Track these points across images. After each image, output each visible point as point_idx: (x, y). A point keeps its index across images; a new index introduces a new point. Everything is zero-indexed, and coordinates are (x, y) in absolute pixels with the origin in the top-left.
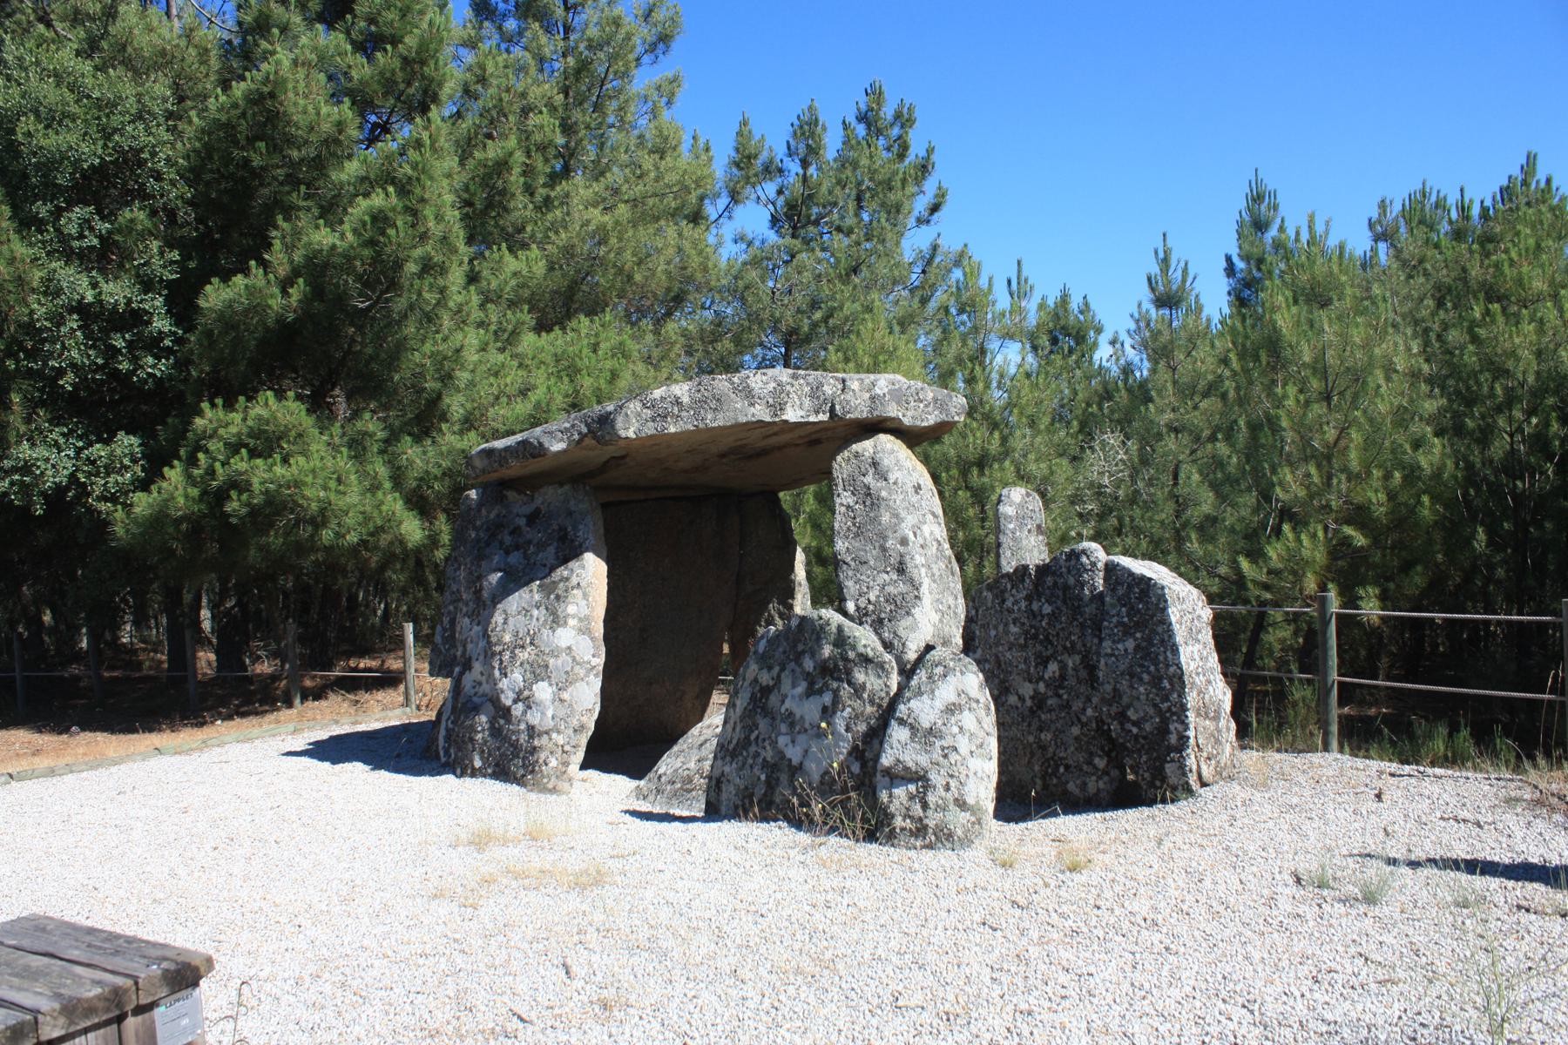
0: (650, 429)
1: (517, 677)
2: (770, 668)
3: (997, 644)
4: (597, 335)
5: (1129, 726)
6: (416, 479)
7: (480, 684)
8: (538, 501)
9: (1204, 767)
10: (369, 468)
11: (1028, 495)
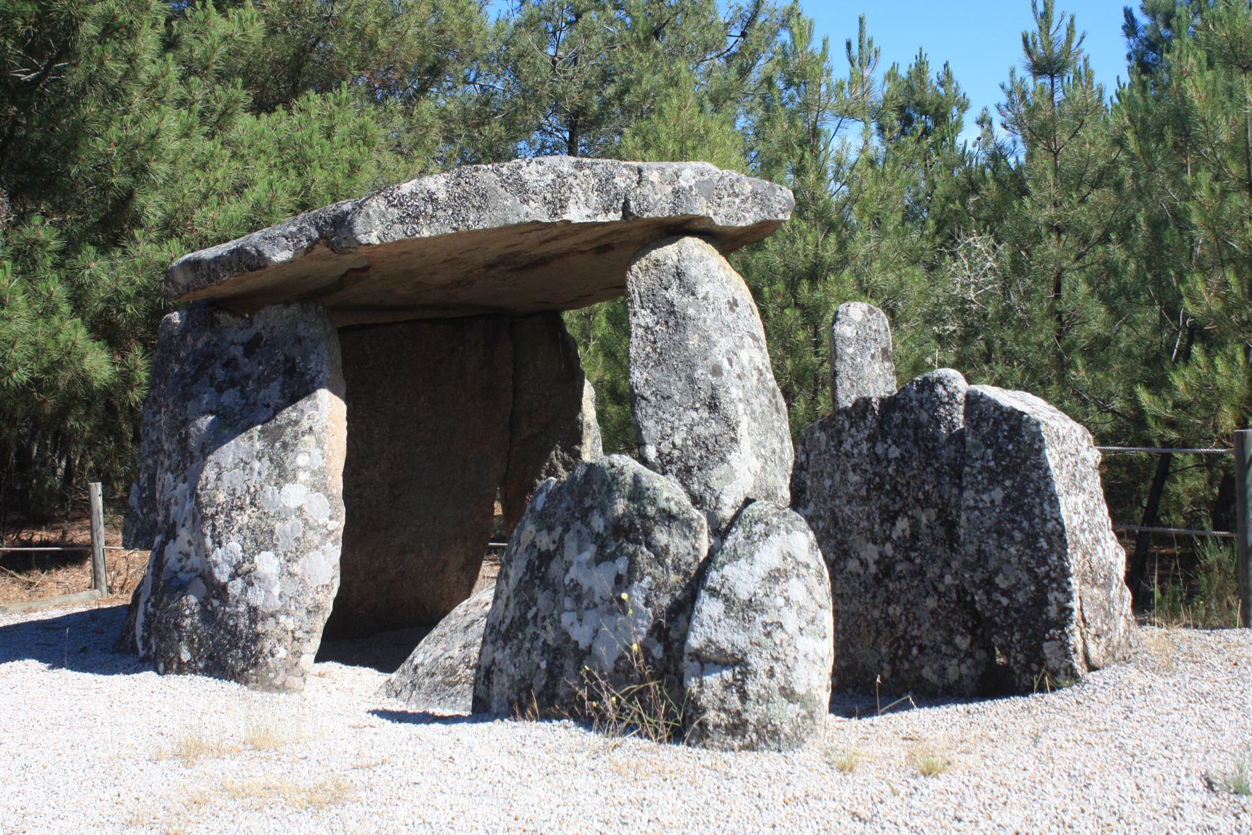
0: (398, 233)
1: (234, 546)
2: (550, 529)
3: (834, 497)
4: (331, 117)
5: (997, 596)
6: (102, 300)
7: (188, 556)
8: (259, 325)
9: (1092, 648)
10: (41, 287)
11: (871, 311)
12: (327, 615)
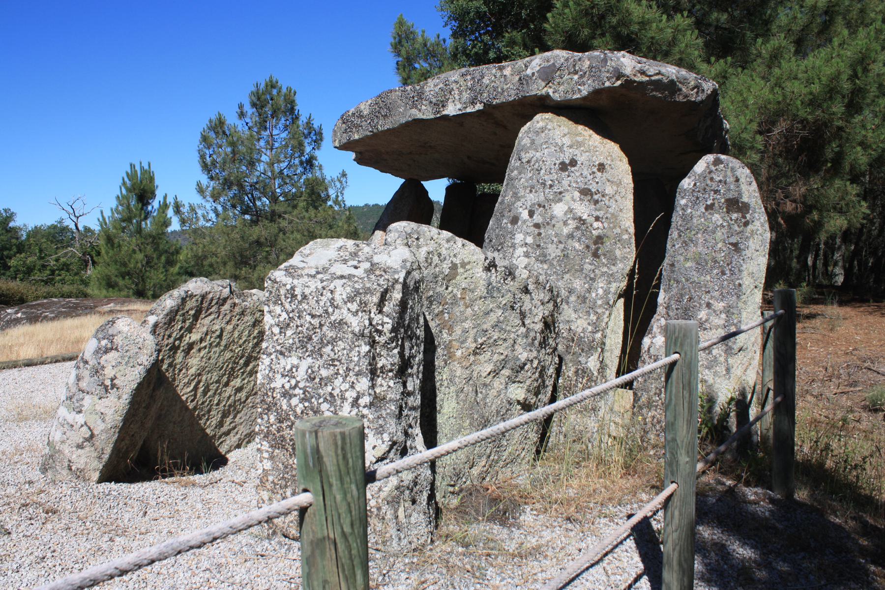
11: (717, 162)
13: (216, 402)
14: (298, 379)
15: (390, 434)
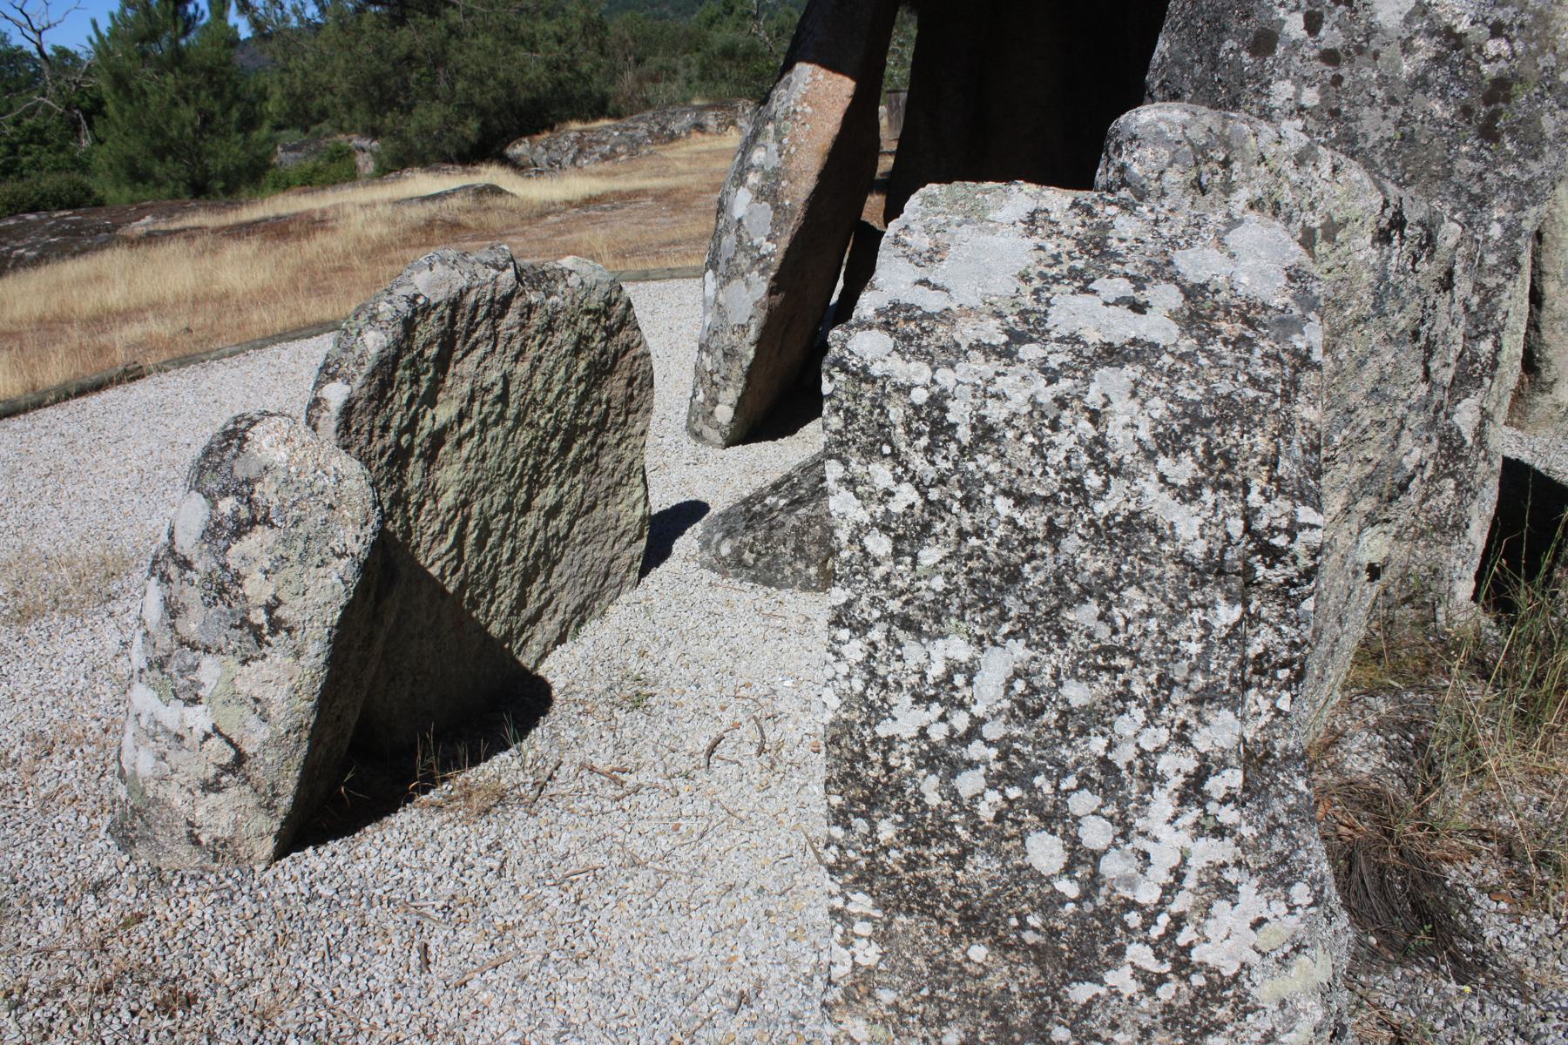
12: (746, 363)
13: (505, 556)
14: (978, 710)
15: (1312, 882)
